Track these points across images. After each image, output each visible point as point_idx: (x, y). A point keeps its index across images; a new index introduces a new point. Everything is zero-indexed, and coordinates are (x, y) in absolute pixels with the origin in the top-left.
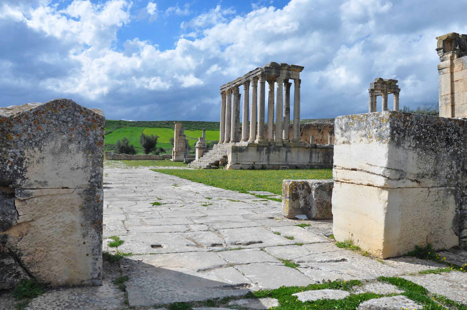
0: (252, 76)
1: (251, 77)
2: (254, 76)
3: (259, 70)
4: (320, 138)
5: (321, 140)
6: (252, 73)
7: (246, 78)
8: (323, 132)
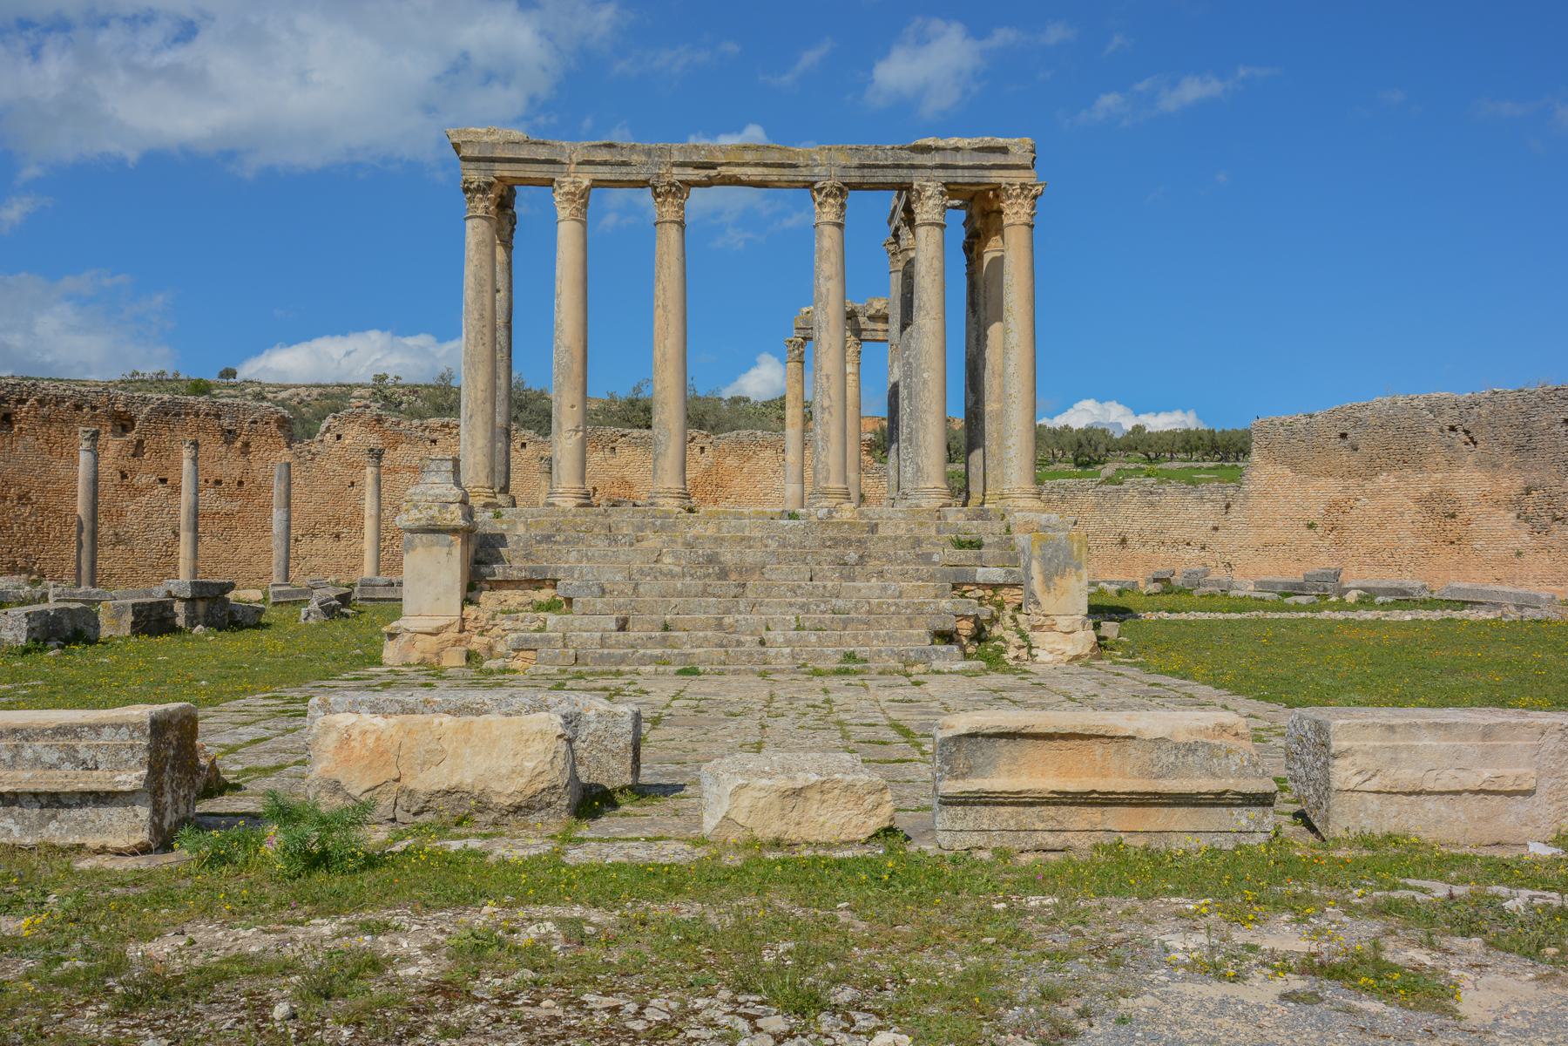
0: (940, 172)
1: (928, 172)
2: (962, 177)
3: (1010, 160)
4: (237, 473)
5: (241, 483)
6: (937, 159)
7: (862, 167)
8: (246, 445)
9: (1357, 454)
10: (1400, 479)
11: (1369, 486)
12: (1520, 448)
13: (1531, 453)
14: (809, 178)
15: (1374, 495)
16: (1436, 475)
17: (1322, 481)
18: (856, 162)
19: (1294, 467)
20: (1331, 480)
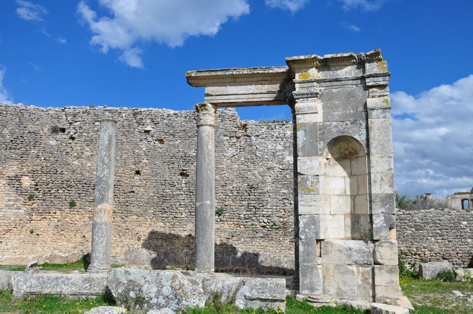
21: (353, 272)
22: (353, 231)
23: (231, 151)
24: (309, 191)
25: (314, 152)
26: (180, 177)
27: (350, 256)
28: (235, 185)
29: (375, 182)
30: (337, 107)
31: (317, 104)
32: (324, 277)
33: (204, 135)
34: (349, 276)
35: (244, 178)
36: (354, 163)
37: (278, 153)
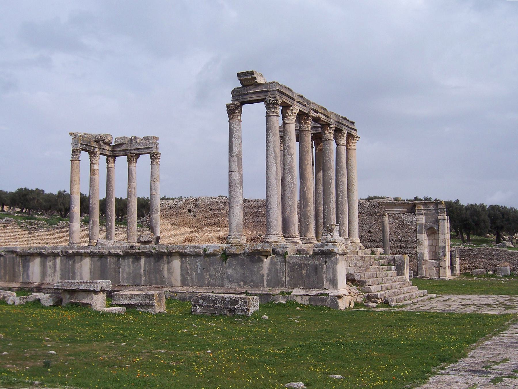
2: (349, 132)
9: (196, 218)
10: (212, 229)
11: (200, 231)
12: (255, 221)
13: (259, 223)
14: (329, 122)
15: (203, 235)
16: (225, 229)
17: (183, 229)
18: (337, 120)
19: (172, 223)
20: (186, 228)
21: (434, 269)
22: (435, 257)
23: (392, 221)
24: (421, 245)
25: (421, 233)
26: (368, 233)
27: (433, 264)
28: (394, 237)
29: (440, 242)
30: (429, 218)
31: (423, 217)
32: (425, 271)
33: (385, 224)
34: (433, 270)
35: (398, 234)
36: (435, 235)
37: (414, 222)
